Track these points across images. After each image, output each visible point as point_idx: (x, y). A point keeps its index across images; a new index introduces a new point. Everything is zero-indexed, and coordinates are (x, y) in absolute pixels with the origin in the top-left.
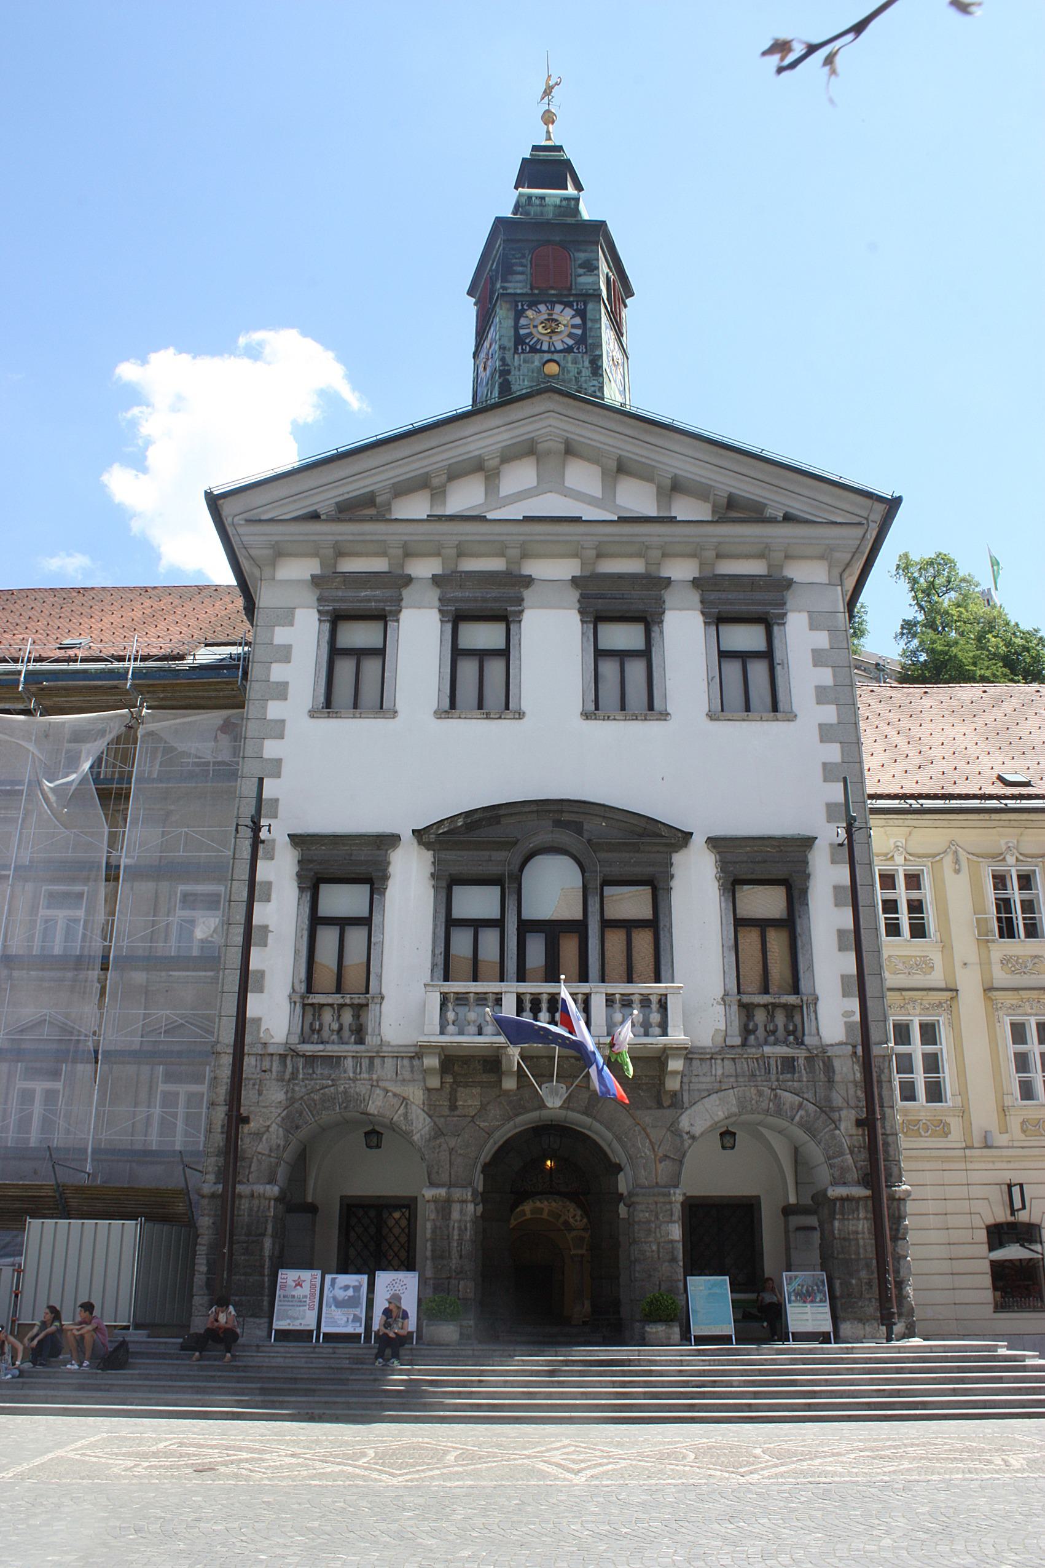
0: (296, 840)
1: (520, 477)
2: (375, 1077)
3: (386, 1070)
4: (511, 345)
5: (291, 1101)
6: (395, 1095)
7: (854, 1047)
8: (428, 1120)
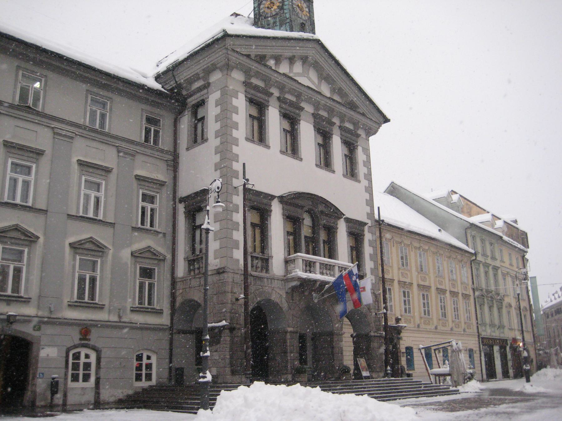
1: (298, 67)
3: (276, 284)
4: (291, 9)
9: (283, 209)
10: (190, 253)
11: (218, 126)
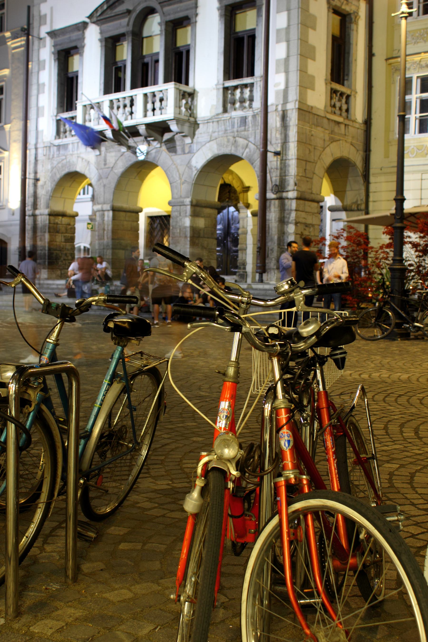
0: (52, 34)
2: (79, 152)
5: (53, 168)
6: (86, 160)
7: (277, 106)
8: (97, 171)
9: (101, 33)
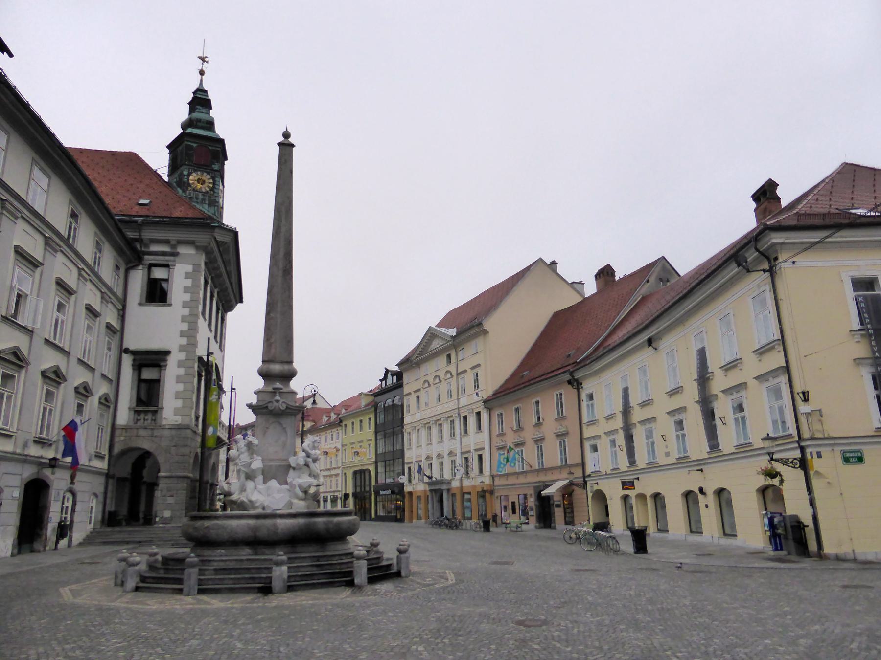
10: (134, 405)
11: (187, 297)
